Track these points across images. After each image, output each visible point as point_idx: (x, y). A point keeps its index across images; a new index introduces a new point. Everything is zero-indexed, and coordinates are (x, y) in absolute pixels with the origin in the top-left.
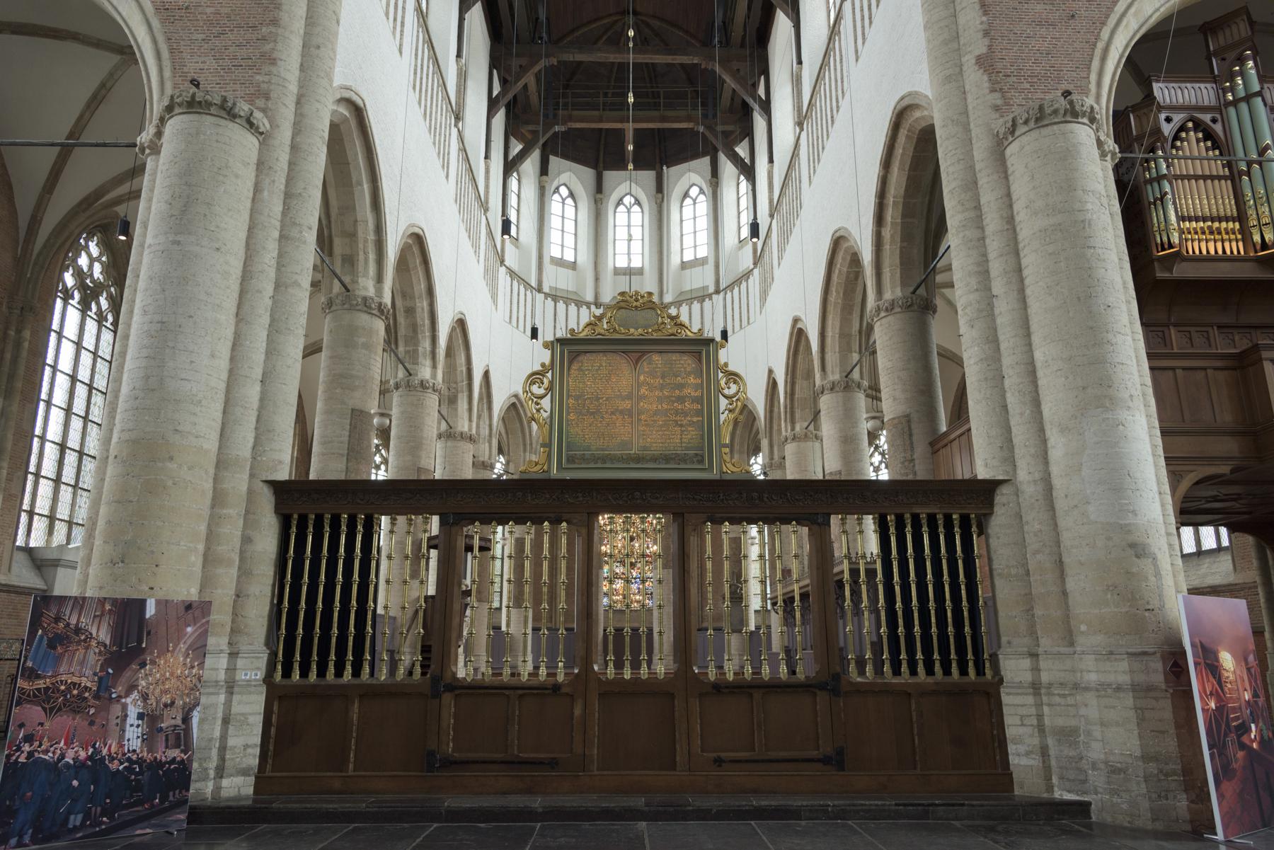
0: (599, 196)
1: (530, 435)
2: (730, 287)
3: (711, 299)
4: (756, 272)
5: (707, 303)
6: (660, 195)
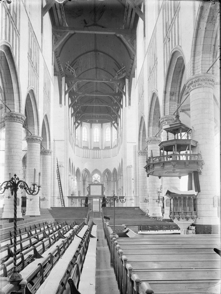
0: (91, 129)
5: (110, 150)
6: (102, 129)
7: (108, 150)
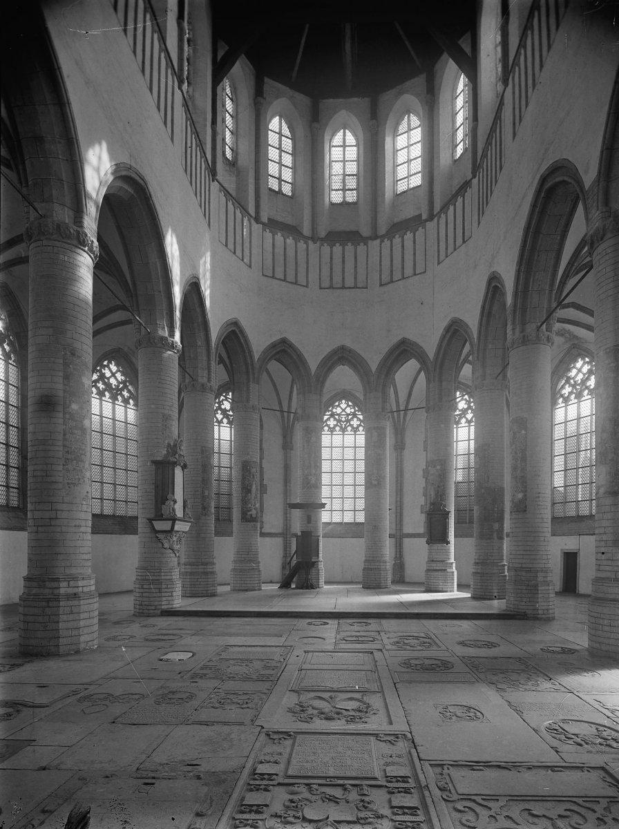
1: (252, 365)
2: (444, 208)
3: (424, 227)
4: (475, 181)
7: (409, 235)
